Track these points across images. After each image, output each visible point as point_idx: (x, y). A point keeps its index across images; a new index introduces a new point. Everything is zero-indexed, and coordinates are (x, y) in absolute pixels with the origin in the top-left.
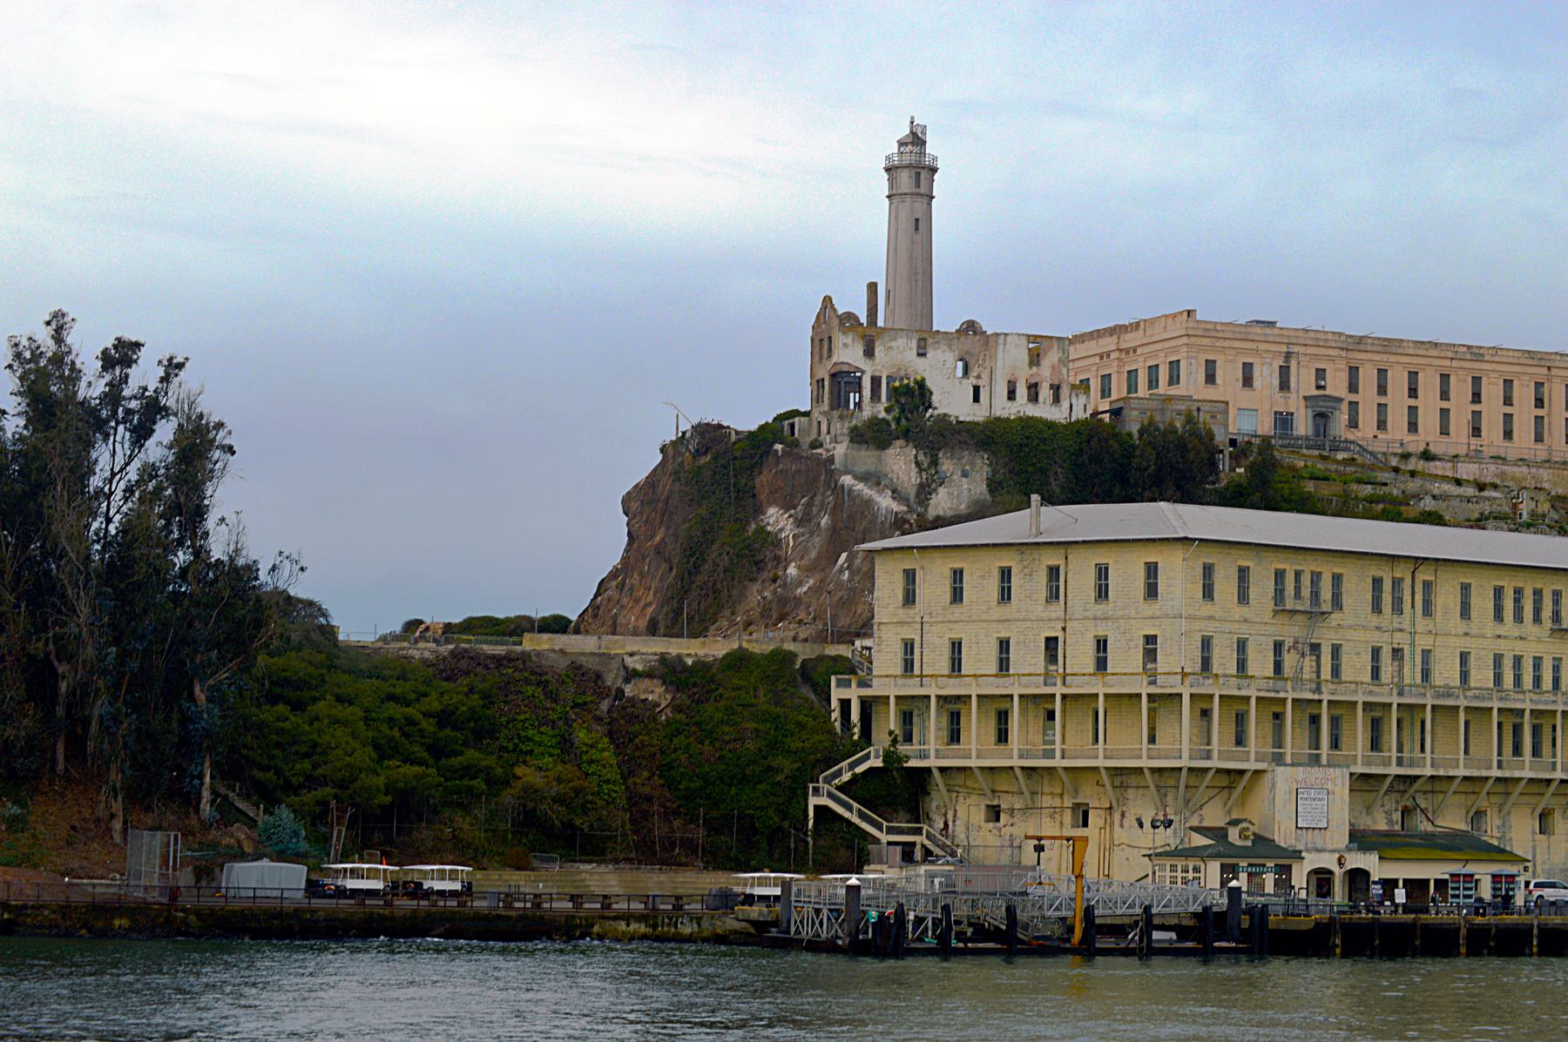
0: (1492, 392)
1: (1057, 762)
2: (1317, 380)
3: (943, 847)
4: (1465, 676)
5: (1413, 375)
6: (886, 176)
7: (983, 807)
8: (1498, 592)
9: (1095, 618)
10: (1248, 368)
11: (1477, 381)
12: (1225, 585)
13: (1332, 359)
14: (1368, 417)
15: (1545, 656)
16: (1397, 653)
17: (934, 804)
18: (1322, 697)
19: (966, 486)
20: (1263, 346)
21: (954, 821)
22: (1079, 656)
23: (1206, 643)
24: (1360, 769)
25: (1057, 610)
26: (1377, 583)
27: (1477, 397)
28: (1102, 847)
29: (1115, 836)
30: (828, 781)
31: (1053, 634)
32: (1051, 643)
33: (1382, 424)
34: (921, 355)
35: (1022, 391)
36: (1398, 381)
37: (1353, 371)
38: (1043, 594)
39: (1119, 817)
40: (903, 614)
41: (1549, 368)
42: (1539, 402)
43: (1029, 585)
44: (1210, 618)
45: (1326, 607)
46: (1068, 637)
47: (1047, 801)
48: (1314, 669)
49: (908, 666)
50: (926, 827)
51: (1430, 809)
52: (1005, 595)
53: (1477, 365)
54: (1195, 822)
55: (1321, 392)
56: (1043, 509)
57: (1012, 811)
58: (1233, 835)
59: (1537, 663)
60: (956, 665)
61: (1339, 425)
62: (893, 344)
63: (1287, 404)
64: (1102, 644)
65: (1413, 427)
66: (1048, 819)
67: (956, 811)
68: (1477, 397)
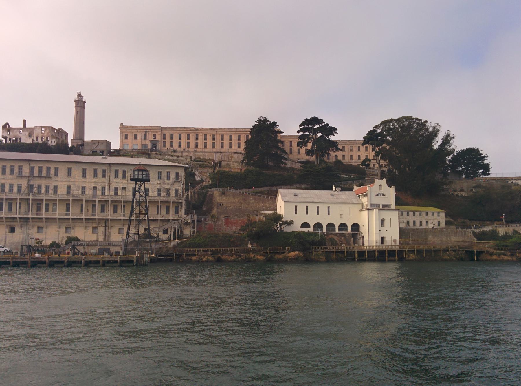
13: (157, 132)
15: (14, 183)
20: (140, 130)
36: (176, 137)
41: (216, 131)
42: (214, 139)
53: (197, 132)
59: (11, 186)
61: (159, 146)
62: (14, 131)
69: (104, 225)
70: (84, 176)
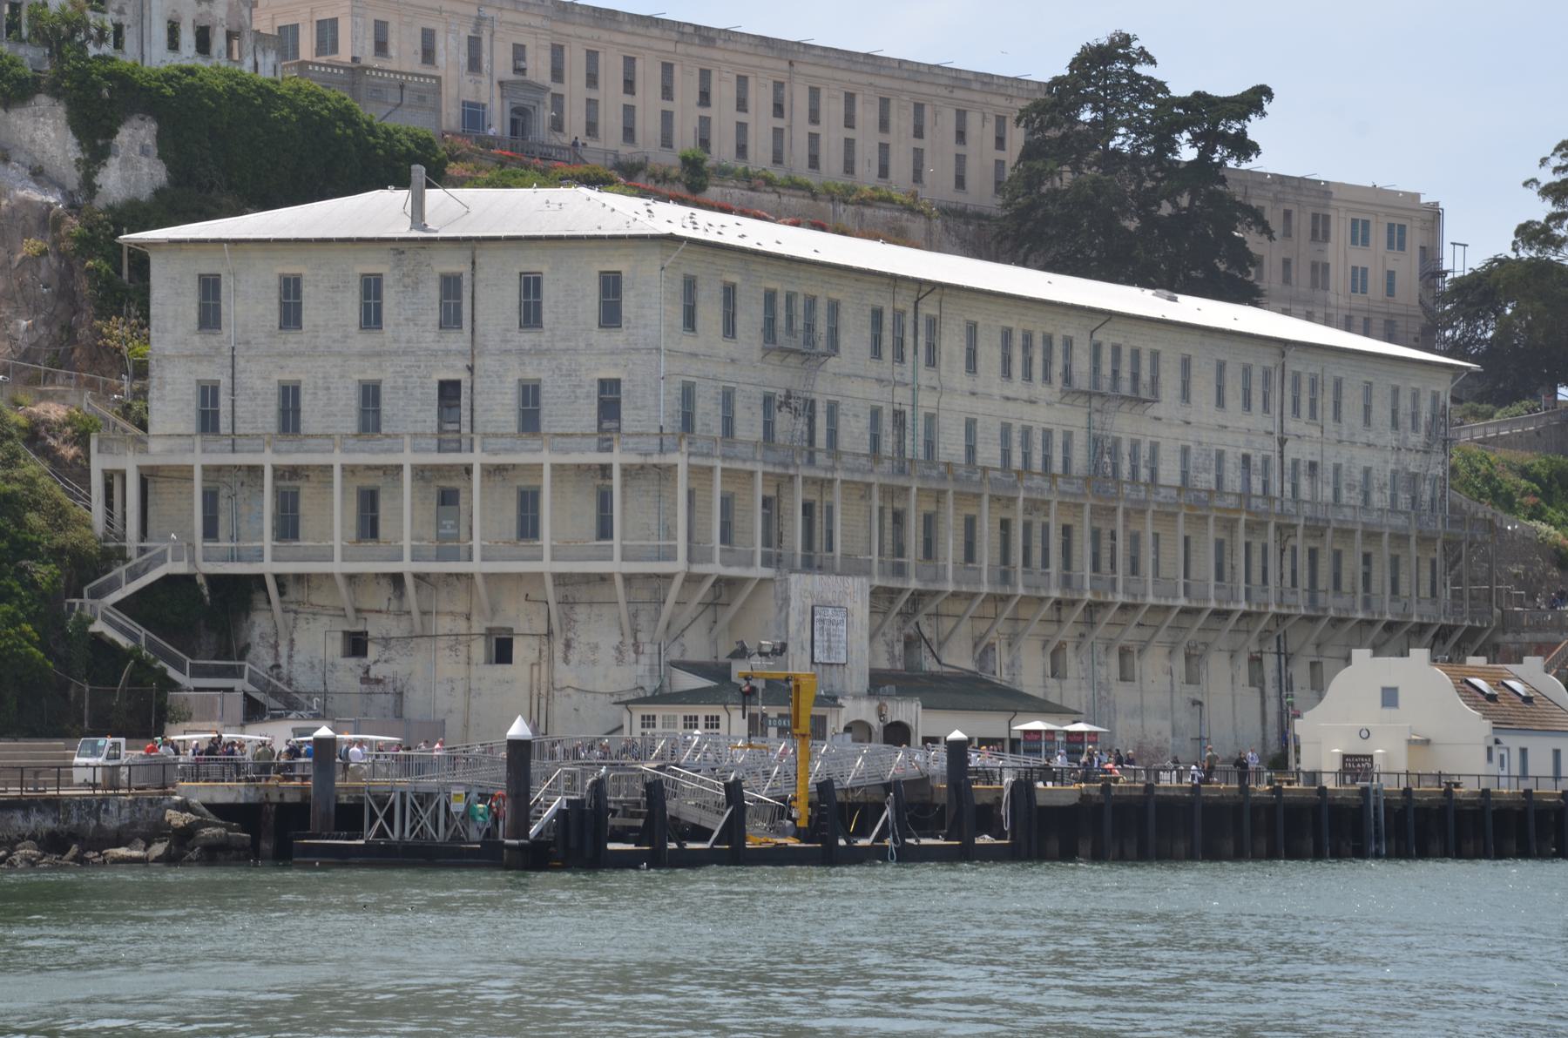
0: (723, 91)
1: (476, 566)
2: (514, 61)
3: (275, 694)
4: (971, 450)
5: (630, 62)
7: (339, 635)
8: (1007, 335)
9: (521, 352)
10: (428, 37)
11: (705, 75)
12: (710, 313)
15: (1054, 427)
16: (899, 416)
17: (256, 632)
18: (835, 476)
19: (146, 170)
21: (290, 657)
23: (688, 393)
24: (877, 582)
26: (877, 315)
27: (705, 98)
28: (535, 691)
29: (557, 676)
30: (98, 594)
31: (451, 376)
32: (449, 392)
35: (187, 38)
37: (557, 52)
38: (434, 316)
39: (562, 647)
40: (197, 339)
42: (778, 110)
44: (694, 355)
45: (822, 346)
46: (477, 381)
48: (806, 437)
49: (208, 421)
50: (248, 665)
51: (935, 640)
52: (371, 318)
54: (675, 655)
55: (519, 77)
56: (429, 193)
58: (739, 668)
59: (1048, 434)
63: (478, 91)
64: (530, 395)
65: (629, 134)
66: (447, 652)
67: (292, 641)
68: (705, 98)
69: (1274, 649)
70: (1220, 402)
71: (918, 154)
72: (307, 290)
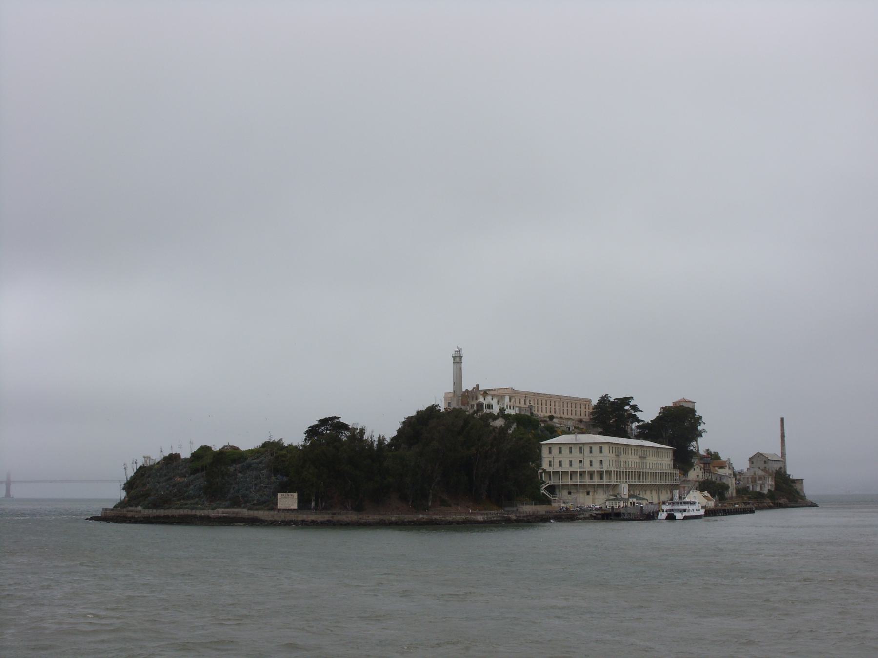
6: (452, 358)
13: (531, 398)
14: (536, 410)
22: (587, 463)
25: (582, 455)
31: (581, 459)
32: (581, 461)
33: (538, 411)
34: (492, 399)
40: (549, 456)
43: (576, 451)
47: (581, 490)
52: (571, 452)
57: (573, 493)
60: (560, 465)
64: (591, 461)
71: (576, 411)
72: (562, 449)
